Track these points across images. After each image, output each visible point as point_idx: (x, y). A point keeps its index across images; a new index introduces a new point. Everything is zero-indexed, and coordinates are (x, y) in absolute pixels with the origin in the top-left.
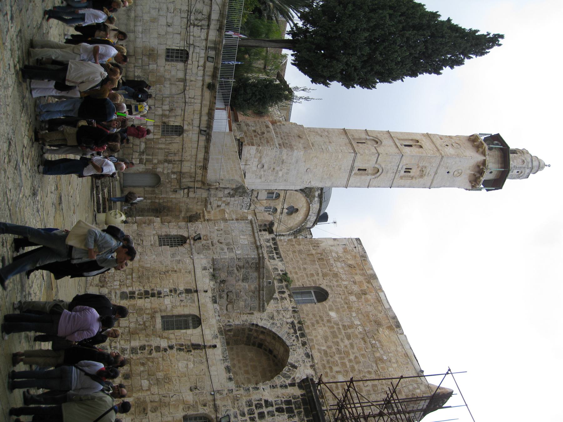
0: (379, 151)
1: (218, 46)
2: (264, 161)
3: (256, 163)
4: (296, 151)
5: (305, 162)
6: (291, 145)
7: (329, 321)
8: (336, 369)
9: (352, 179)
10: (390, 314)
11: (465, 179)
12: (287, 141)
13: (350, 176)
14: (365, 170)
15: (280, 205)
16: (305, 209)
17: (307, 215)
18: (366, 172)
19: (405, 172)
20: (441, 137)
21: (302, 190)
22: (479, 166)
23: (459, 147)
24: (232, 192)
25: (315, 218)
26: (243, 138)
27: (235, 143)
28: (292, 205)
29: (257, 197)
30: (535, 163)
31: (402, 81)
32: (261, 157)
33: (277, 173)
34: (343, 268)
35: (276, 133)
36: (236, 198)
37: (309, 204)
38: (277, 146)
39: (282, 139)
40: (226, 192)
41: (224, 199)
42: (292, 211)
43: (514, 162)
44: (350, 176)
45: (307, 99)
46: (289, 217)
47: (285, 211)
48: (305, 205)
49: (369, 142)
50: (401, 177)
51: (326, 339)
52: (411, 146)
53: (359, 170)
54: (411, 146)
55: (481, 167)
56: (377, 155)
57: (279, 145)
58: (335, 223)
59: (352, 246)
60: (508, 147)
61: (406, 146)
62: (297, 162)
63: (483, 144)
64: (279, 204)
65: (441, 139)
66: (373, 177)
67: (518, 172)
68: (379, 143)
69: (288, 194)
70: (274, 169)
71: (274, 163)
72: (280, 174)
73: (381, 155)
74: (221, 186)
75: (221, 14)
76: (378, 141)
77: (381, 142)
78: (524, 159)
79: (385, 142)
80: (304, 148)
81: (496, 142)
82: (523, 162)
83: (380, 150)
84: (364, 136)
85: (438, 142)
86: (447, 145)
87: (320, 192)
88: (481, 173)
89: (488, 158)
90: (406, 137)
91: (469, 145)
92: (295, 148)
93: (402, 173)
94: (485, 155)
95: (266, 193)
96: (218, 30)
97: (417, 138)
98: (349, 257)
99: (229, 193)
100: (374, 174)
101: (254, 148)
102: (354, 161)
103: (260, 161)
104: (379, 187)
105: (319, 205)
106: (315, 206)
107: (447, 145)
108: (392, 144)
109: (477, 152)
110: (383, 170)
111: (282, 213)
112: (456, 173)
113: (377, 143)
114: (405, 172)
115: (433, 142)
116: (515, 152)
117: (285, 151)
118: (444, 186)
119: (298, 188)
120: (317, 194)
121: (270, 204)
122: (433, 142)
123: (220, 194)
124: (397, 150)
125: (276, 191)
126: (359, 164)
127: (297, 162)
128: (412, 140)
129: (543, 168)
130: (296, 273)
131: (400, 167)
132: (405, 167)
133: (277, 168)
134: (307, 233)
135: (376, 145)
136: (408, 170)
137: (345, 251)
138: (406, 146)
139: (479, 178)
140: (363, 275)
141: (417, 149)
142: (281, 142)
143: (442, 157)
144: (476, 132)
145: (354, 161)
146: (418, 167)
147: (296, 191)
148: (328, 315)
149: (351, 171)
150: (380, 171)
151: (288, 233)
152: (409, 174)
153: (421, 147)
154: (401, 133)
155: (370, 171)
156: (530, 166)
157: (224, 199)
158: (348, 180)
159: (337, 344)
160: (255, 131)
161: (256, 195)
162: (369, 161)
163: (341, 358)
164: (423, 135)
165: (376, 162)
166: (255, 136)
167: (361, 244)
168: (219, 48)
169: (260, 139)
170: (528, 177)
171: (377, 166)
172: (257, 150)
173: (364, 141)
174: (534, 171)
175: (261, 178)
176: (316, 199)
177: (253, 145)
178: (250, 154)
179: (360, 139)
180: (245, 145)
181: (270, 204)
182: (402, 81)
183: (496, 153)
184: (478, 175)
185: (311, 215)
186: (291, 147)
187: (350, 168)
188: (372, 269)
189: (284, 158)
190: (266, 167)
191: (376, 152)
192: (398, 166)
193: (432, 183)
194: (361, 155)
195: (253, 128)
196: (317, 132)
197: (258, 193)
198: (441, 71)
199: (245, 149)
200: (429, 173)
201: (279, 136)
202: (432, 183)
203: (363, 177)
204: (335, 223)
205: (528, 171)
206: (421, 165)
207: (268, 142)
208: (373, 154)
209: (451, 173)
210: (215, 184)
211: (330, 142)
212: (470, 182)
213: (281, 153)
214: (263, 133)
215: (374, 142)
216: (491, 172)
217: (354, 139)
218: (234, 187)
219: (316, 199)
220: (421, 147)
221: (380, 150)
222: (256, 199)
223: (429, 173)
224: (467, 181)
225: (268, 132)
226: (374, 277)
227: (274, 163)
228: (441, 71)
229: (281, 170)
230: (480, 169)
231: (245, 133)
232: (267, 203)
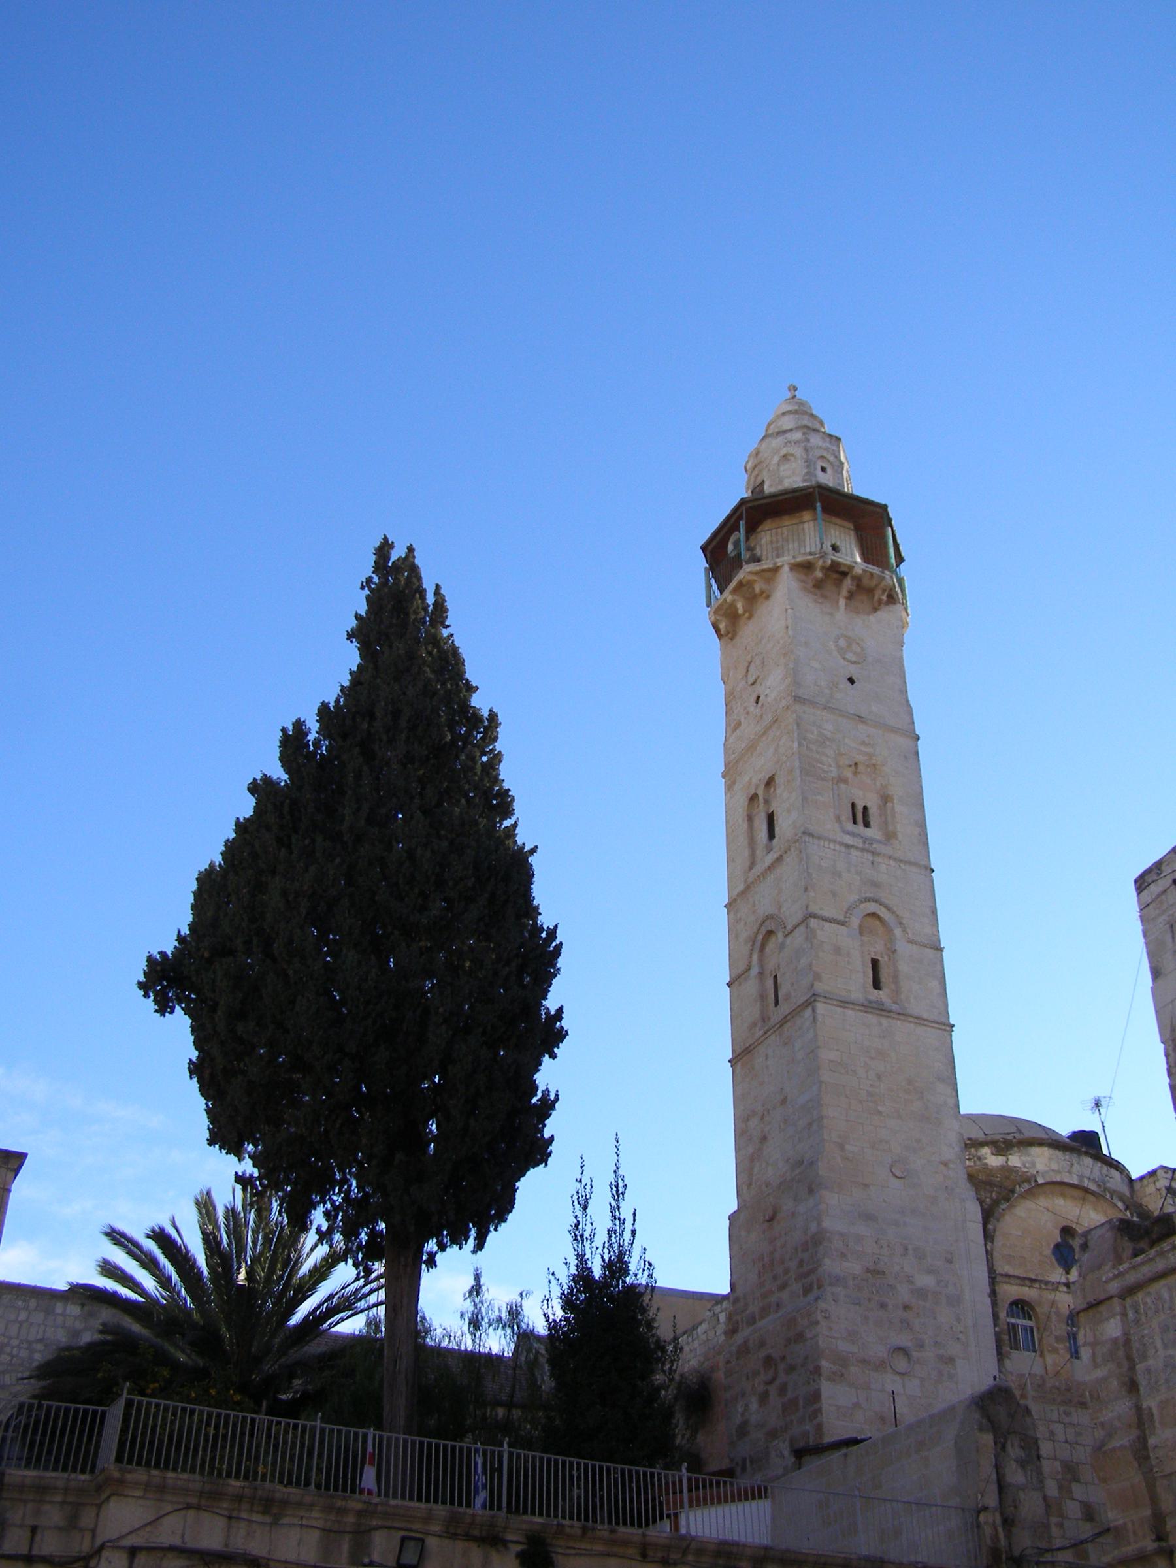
0: (800, 916)
1: (351, 1519)
2: (879, 1351)
3: (890, 1382)
4: (827, 1223)
5: (866, 1186)
6: (805, 1247)
9: (915, 1008)
11: (869, 627)
12: (793, 1265)
13: (903, 1015)
14: (875, 964)
16: (1060, 1201)
17: (1082, 1192)
18: (883, 960)
19: (867, 824)
20: (733, 726)
21: (988, 1215)
22: (818, 585)
23: (758, 661)
24: (1014, 1451)
25: (1088, 1161)
26: (792, 1441)
27: (813, 1464)
28: (1048, 1252)
30: (788, 423)
31: (533, 850)
32: (864, 1361)
33: (921, 1293)
35: (765, 1311)
36: (1041, 1432)
38: (811, 1297)
39: (783, 1287)
40: (1015, 1476)
41: (1052, 1489)
43: (791, 477)
44: (903, 1015)
45: (618, 1192)
48: (1043, 1202)
49: (771, 965)
50: (890, 836)
52: (771, 819)
53: (877, 985)
54: (771, 819)
55: (819, 574)
56: (813, 923)
57: (807, 1290)
58: (1097, 1105)
60: (743, 502)
61: (771, 835)
62: (869, 1217)
63: (740, 584)
65: (739, 724)
66: (898, 932)
67: (823, 470)
68: (770, 925)
69: (1007, 1269)
70: (906, 1307)
71: (883, 1306)
72: (925, 1281)
73: (814, 908)
74: (992, 1500)
75: (207, 1500)
76: (764, 930)
77: (769, 917)
78: (776, 459)
79: (765, 906)
80: (811, 1191)
81: (730, 547)
82: (785, 457)
83: (792, 913)
84: (751, 987)
85: (749, 729)
87: (986, 1151)
88: (837, 572)
89: (785, 560)
90: (743, 840)
91: (748, 631)
92: (813, 1227)
93: (872, 832)
94: (776, 570)
95: (1015, 1354)
96: (275, 1523)
97: (742, 800)
99: (1022, 1464)
100: (889, 931)
101: (827, 1389)
102: (845, 1003)
103: (880, 1366)
104: (934, 912)
105: (1035, 1150)
106: (1041, 1162)
108: (771, 877)
109: (768, 597)
110: (868, 900)
112: (849, 656)
113: (770, 933)
114: (867, 824)
115: (751, 747)
116: (758, 488)
117: (830, 1266)
118: (904, 691)
119: (974, 1211)
120: (994, 1161)
122: (751, 747)
123: (1030, 1506)
124: (791, 859)
125: (1003, 1314)
126: (857, 983)
127: (869, 1217)
128: (750, 818)
129: (802, 404)
131: (848, 840)
132: (850, 826)
133: (904, 1293)
134: (1151, 1189)
135: (780, 935)
136: (861, 816)
138: (771, 835)
139: (858, 580)
141: (778, 792)
142: (796, 1287)
143: (797, 699)
144: (702, 617)
145: (845, 1003)
146: (845, 781)
147: (988, 1236)
149: (879, 1009)
150: (872, 907)
152: (873, 811)
153: (770, 782)
154: (730, 861)
155: (877, 948)
156: (798, 435)
157: (1052, 1489)
158: (920, 1020)
160: (764, 1398)
162: (837, 950)
164: (729, 787)
165: (842, 923)
166: (783, 1390)
168: (360, 1513)
169: (791, 1369)
170: (838, 439)
171: (855, 922)
172: (838, 1377)
173: (770, 982)
174: (817, 426)
175: (951, 1360)
176: (1015, 1160)
177: (816, 1396)
178: (857, 1405)
179: (762, 997)
180: (819, 1427)
182: (533, 850)
183: (766, 537)
184: (848, 583)
185: (1081, 1177)
186: (815, 1242)
187: (872, 1019)
189: (854, 1267)
190: (904, 1340)
191: (802, 928)
192: (848, 846)
193: (894, 730)
194: (817, 977)
195: (754, 1406)
196: (752, 1160)
198: (485, 713)
199: (836, 1428)
200: (863, 743)
201: (773, 1299)
202: (894, 730)
203: (903, 967)
204: (1097, 1105)
205: (815, 440)
206: (834, 772)
207: (800, 1337)
208: (810, 936)
209: (853, 671)
210: (988, 1531)
211: (784, 1101)
212: (875, 610)
213: (838, 1280)
214: (769, 1361)
215: (770, 946)
216: (835, 548)
217: (764, 1019)
218: (988, 1438)
219: (1015, 1160)
220: (770, 782)
221: (792, 913)
223: (863, 743)
224: (872, 618)
225: (762, 1344)
227: (883, 1306)
228: (485, 713)
229: (909, 1280)
230: (828, 578)
231: (773, 1434)
232: (1055, 1350)
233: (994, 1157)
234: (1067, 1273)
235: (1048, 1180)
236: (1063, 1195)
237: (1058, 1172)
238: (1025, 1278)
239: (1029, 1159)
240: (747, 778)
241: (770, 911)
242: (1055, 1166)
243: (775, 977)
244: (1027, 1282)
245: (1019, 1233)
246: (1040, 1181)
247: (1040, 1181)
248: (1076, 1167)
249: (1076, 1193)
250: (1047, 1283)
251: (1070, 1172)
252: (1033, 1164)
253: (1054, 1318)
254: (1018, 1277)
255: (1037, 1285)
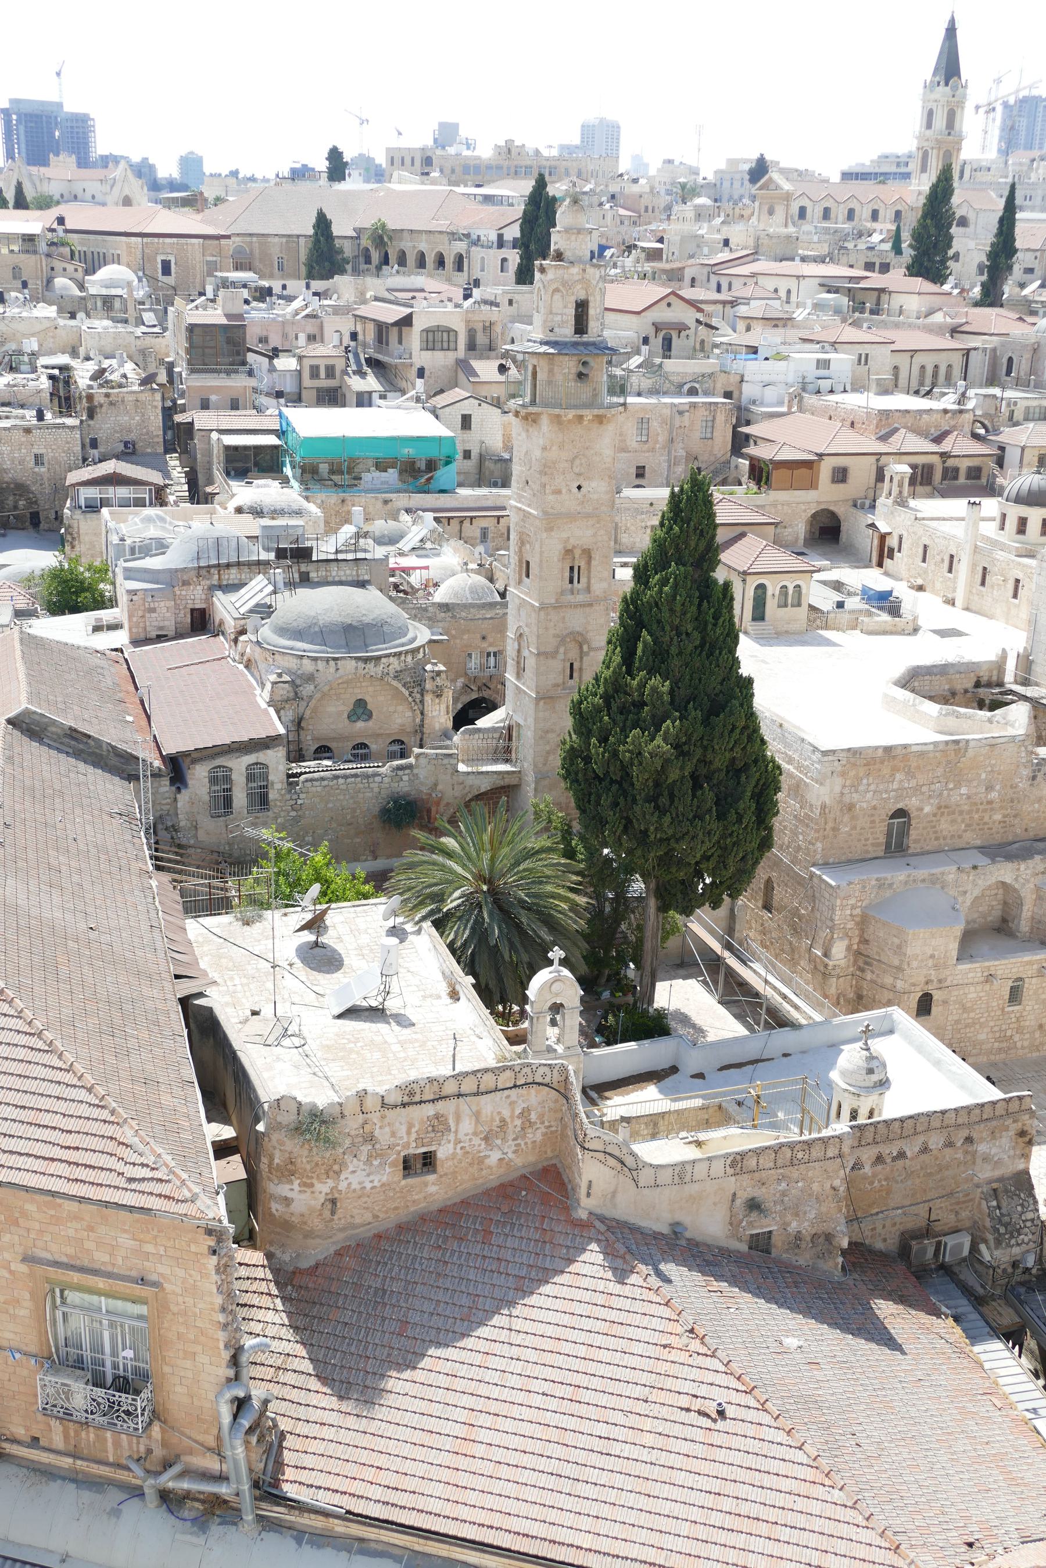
7: (935, 815)
8: (986, 819)
10: (941, 747)
34: (869, 785)
51: (953, 821)
59: (836, 763)
84: (558, 665)
86: (579, 487)
98: (852, 773)
107: (579, 487)
130: (867, 840)
137: (843, 774)
140: (882, 763)
148: (927, 815)
159: (961, 813)
163: (977, 811)
167: (834, 752)
188: (877, 748)
226: (888, 749)
240: (565, 535)
241: (578, 629)
243: (572, 665)
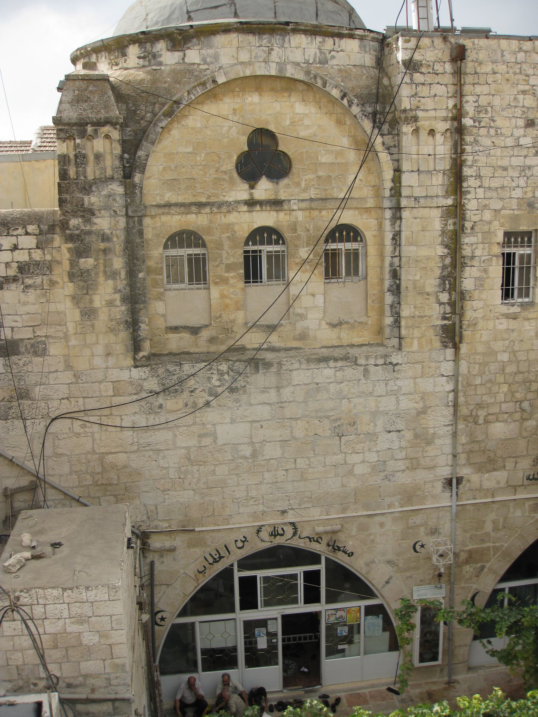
15: (232, 218)
16: (254, 98)
28: (230, 165)
29: (195, 331)
37: (213, 90)
42: (263, 157)
46: (296, 167)
47: (264, 188)
48: (226, 105)
64: (229, 227)
87: (161, 46)
105: (220, 39)
111: (276, 204)
121: (229, 268)
151: (384, 156)
161: (186, 336)
181: (229, 268)
185: (281, 66)
197: (175, 329)
219: (193, 55)
222: (205, 334)
232: (225, 281)
233: (169, 53)
234: (252, 187)
235: (232, 77)
236: (259, 89)
237: (250, 63)
238: (192, 204)
239: (211, 51)
242: (244, 56)
244: (193, 209)
245: (190, 150)
246: (221, 80)
247: (221, 80)
248: (274, 56)
249: (278, 84)
250: (220, 205)
251: (266, 62)
252: (216, 57)
253: (227, 244)
254: (183, 205)
255: (207, 210)
